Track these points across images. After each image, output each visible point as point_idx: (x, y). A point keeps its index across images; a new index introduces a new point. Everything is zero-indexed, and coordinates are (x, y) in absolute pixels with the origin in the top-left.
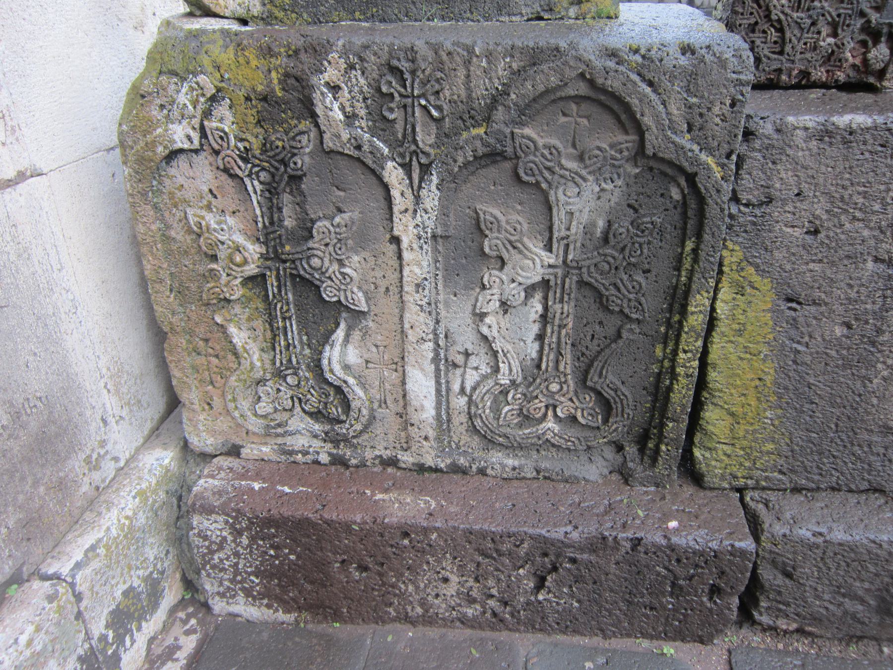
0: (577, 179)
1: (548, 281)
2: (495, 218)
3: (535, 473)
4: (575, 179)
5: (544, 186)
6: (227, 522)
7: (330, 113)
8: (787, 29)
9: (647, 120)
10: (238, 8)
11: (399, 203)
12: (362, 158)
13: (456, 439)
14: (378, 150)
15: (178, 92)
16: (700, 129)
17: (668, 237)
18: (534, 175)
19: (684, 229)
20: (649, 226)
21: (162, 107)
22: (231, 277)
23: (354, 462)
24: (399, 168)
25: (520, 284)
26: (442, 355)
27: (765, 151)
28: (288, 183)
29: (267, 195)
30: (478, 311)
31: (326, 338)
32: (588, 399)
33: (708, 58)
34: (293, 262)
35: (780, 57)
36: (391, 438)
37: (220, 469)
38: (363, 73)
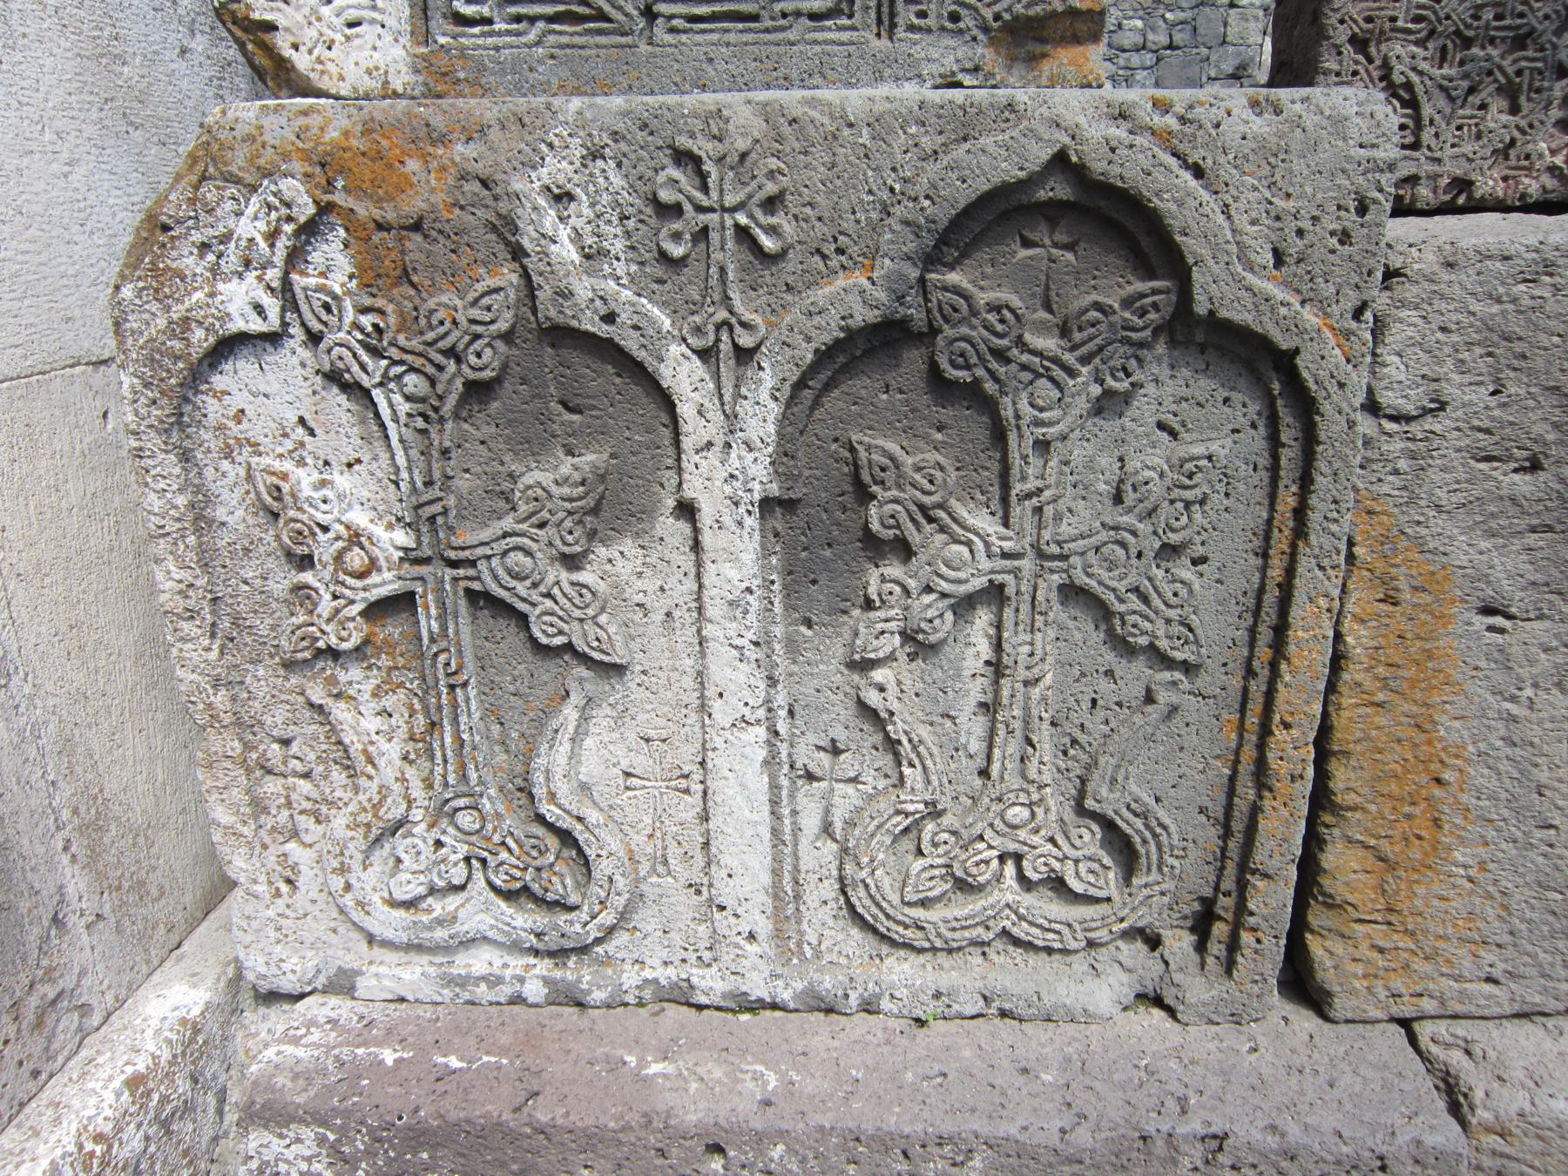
0: (1057, 372)
1: (1002, 587)
2: (892, 458)
3: (981, 1003)
4: (1049, 369)
5: (990, 387)
6: (322, 1141)
7: (553, 248)
8: (1422, 99)
9: (1192, 246)
10: (366, 77)
11: (695, 430)
12: (617, 339)
14: (653, 322)
15: (239, 214)
16: (1299, 261)
17: (1242, 487)
18: (968, 367)
19: (1274, 469)
20: (1204, 463)
21: (204, 247)
22: (342, 601)
23: (598, 996)
24: (694, 357)
25: (944, 595)
26: (784, 756)
27: (1425, 306)
28: (464, 399)
30: (857, 657)
32: (1087, 837)
34: (472, 563)
35: (1416, 154)
37: (311, 1024)
38: (619, 165)
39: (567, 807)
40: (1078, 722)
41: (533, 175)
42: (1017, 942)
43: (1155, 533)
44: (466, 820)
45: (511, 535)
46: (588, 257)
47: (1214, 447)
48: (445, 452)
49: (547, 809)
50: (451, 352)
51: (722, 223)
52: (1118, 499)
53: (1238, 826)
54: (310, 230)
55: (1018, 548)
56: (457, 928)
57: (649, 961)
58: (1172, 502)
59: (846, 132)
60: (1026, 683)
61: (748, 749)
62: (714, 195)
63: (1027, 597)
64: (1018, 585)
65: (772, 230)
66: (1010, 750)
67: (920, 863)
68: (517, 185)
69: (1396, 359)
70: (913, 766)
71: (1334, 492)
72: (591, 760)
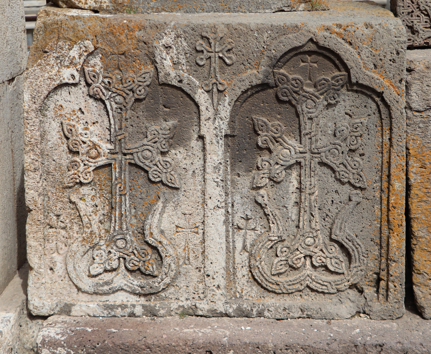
0: (314, 98)
2: (265, 123)
3: (300, 312)
5: (294, 102)
7: (165, 61)
9: (349, 64)
11: (205, 114)
12: (183, 87)
13: (239, 290)
14: (193, 82)
17: (372, 132)
18: (287, 96)
20: (359, 125)
21: (58, 58)
25: (282, 165)
26: (230, 220)
27: (422, 79)
29: (119, 111)
30: (254, 186)
31: (150, 209)
32: (334, 250)
33: (381, 30)
34: (132, 154)
36: (191, 289)
38: (185, 39)
39: (156, 238)
40: (327, 208)
41: (160, 41)
42: (312, 290)
43: (347, 146)
44: (120, 243)
45: (145, 145)
46: (174, 64)
47: (362, 120)
48: (126, 119)
49: (148, 239)
50: (131, 90)
51: (215, 55)
52: (335, 135)
53: (384, 245)
54: (91, 54)
55: (304, 151)
56: (113, 285)
57: (181, 299)
58: (351, 136)
59: (250, 32)
60: (309, 194)
61: (219, 216)
62: (213, 48)
63: (308, 166)
64: (305, 162)
65: (229, 58)
66: (306, 218)
67: (276, 260)
68: (155, 44)
69: (415, 94)
70: (274, 224)
71: (399, 133)
72: (164, 221)
